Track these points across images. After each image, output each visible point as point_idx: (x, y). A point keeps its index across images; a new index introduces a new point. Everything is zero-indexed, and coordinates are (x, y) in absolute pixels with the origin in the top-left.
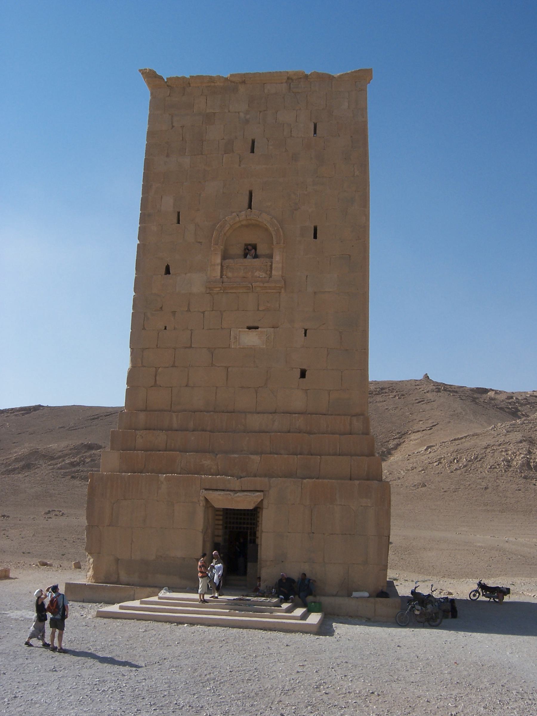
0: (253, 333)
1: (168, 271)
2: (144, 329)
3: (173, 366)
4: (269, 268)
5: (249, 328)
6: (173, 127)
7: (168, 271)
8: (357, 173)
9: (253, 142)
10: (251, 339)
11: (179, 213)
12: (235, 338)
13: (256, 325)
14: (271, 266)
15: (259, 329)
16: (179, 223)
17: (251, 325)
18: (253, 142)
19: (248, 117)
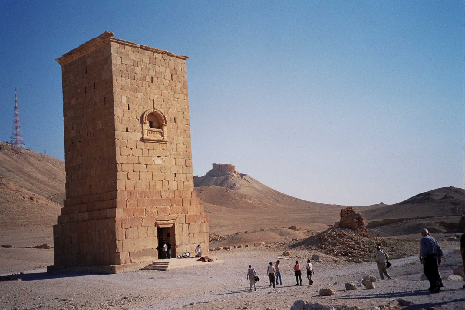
0: (159, 159)
1: (127, 131)
2: (121, 155)
3: (134, 171)
4: (162, 133)
5: (158, 157)
6: (122, 63)
7: (127, 131)
8: (186, 99)
9: (152, 77)
10: (158, 161)
11: (129, 105)
12: (154, 161)
13: (160, 156)
14: (163, 133)
15: (161, 158)
16: (129, 109)
17: (158, 155)
18: (152, 77)
19: (149, 66)
